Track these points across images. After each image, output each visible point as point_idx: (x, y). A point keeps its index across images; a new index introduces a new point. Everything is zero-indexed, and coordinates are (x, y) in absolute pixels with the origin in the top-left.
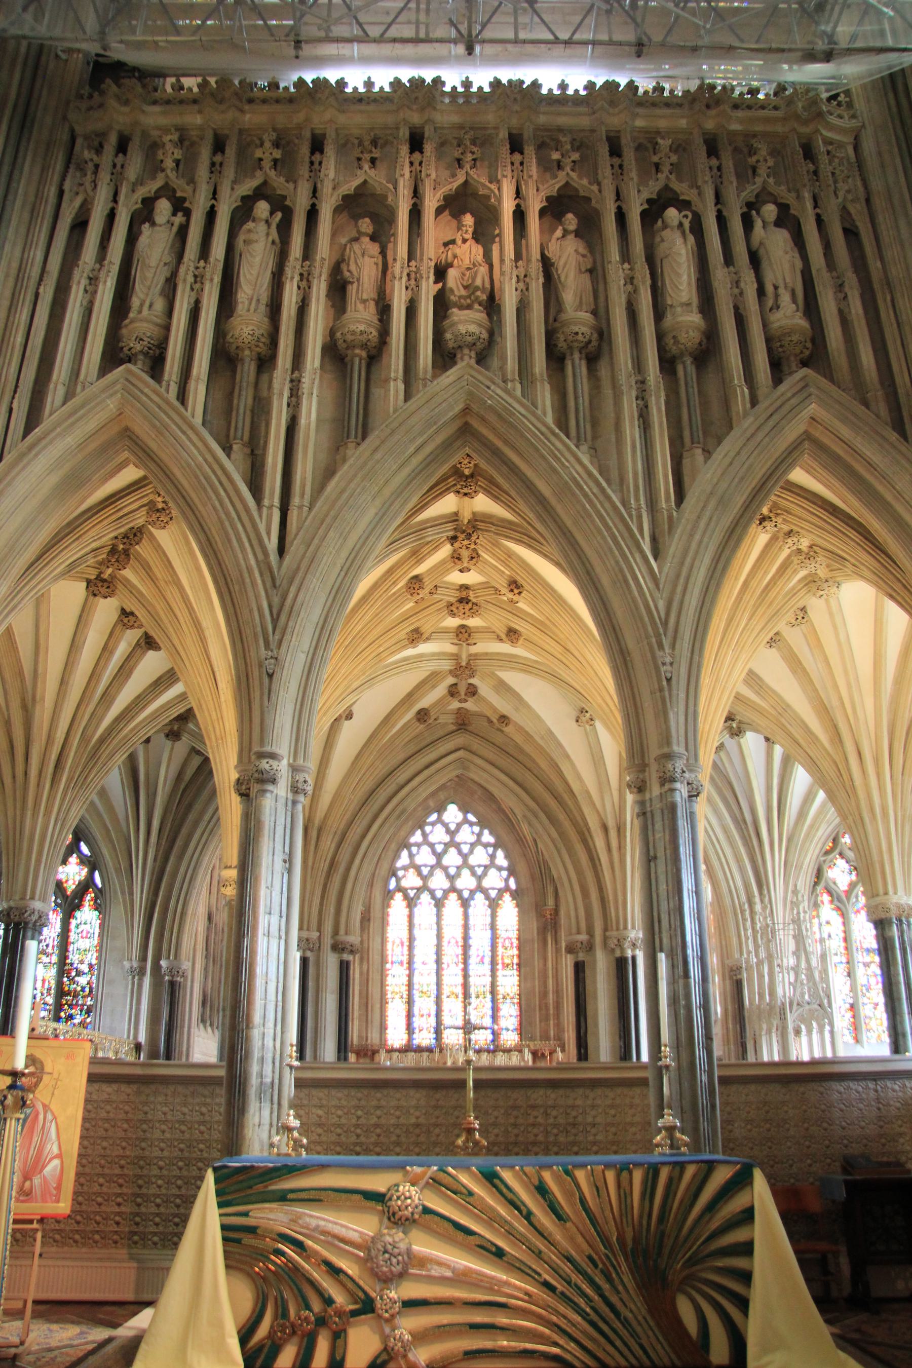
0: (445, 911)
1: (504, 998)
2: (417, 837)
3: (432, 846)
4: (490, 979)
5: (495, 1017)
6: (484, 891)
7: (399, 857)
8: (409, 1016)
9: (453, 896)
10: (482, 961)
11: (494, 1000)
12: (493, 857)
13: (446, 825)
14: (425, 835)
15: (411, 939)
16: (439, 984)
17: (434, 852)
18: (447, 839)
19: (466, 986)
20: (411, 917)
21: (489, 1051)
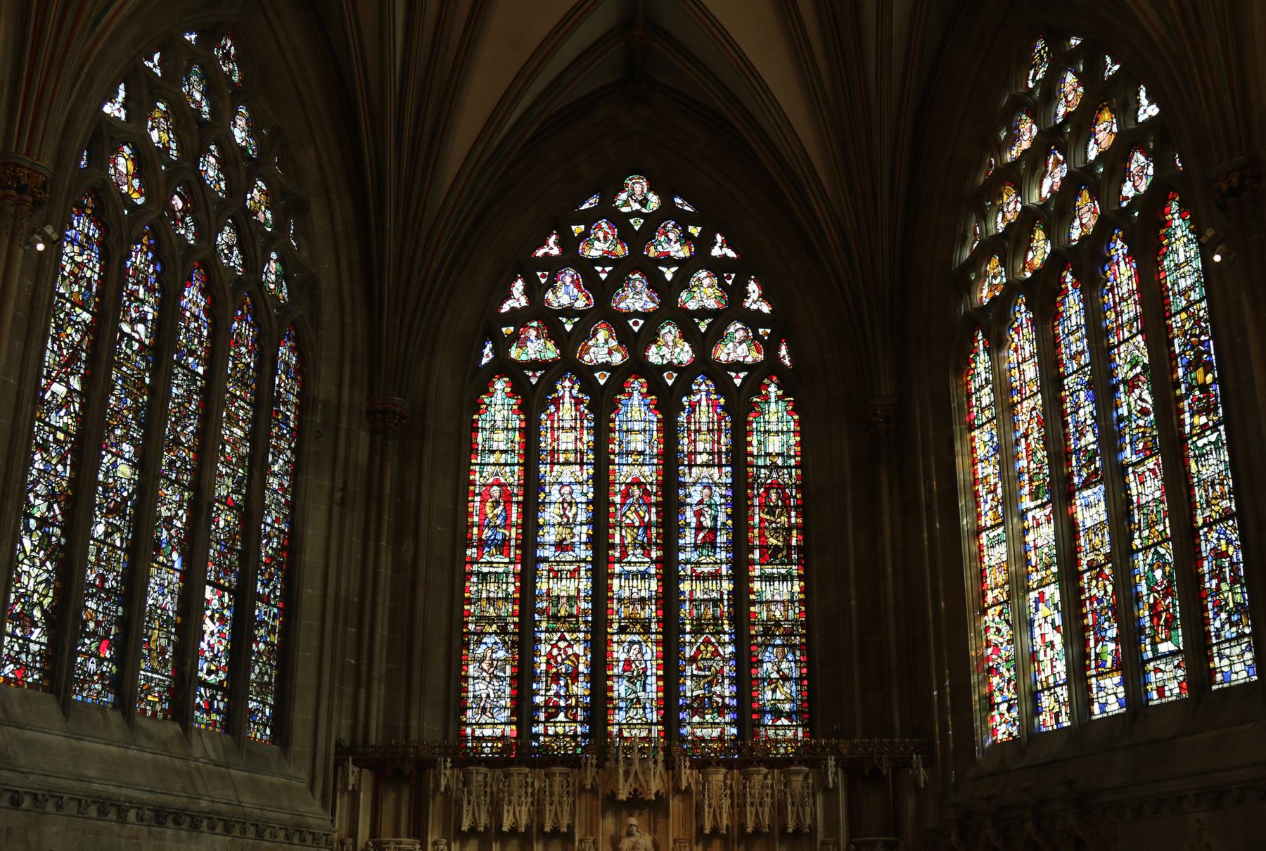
0: (618, 421)
1: (767, 632)
2: (552, 248)
3: (586, 268)
4: (727, 586)
5: (745, 680)
6: (718, 373)
7: (509, 296)
8: (523, 679)
9: (637, 385)
10: (710, 543)
11: (741, 639)
12: (736, 294)
13: (620, 221)
14: (568, 243)
15: (532, 487)
16: (600, 593)
17: (589, 281)
18: (621, 251)
19: (669, 599)
20: (530, 433)
21: (729, 765)
